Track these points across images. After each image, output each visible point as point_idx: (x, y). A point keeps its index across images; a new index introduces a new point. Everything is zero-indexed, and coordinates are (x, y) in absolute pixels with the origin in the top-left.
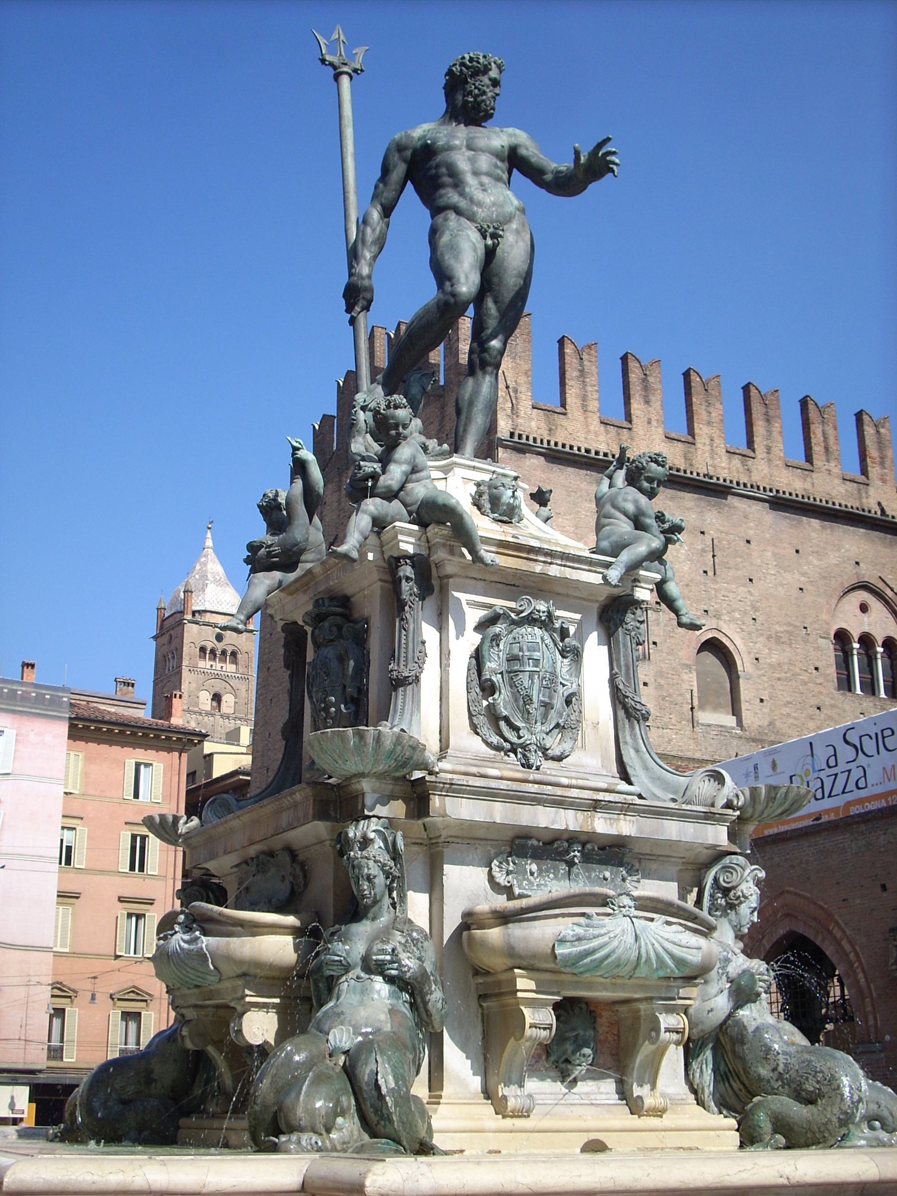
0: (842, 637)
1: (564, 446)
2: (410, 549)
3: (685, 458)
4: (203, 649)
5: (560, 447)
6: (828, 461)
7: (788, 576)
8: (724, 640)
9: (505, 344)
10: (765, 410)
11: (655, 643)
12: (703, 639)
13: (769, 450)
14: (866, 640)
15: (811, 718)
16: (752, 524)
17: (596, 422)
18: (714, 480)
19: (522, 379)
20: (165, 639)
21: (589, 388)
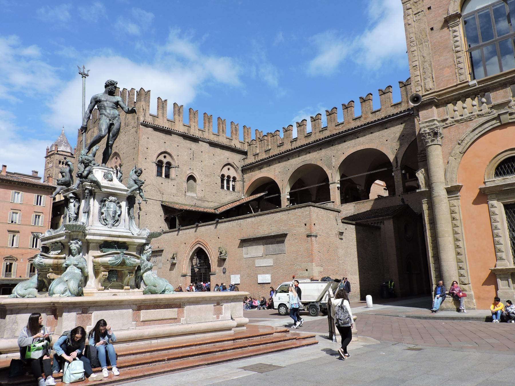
0: (223, 176)
1: (157, 125)
2: (88, 188)
3: (188, 130)
4: (60, 162)
5: (156, 126)
6: (223, 133)
7: (211, 161)
8: (194, 175)
9: (114, 142)
10: (208, 120)
11: (177, 176)
12: (189, 175)
13: (209, 130)
14: (229, 177)
15: (214, 195)
16: (203, 148)
17: (166, 120)
18: (194, 136)
19: (147, 107)
20: (49, 158)
21: (164, 111)
